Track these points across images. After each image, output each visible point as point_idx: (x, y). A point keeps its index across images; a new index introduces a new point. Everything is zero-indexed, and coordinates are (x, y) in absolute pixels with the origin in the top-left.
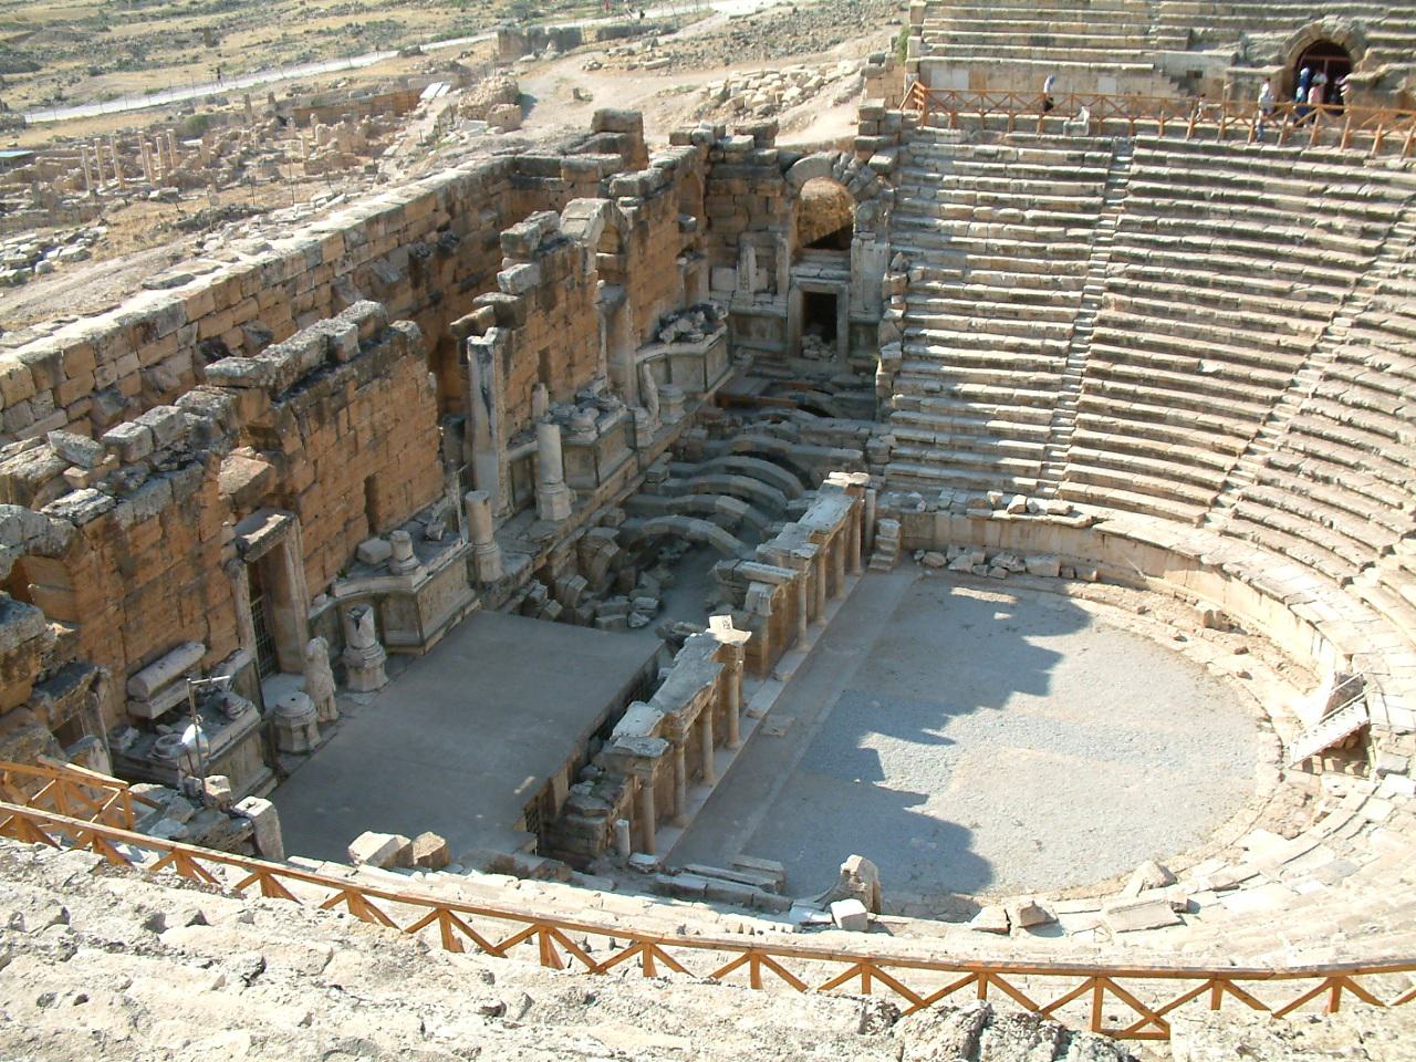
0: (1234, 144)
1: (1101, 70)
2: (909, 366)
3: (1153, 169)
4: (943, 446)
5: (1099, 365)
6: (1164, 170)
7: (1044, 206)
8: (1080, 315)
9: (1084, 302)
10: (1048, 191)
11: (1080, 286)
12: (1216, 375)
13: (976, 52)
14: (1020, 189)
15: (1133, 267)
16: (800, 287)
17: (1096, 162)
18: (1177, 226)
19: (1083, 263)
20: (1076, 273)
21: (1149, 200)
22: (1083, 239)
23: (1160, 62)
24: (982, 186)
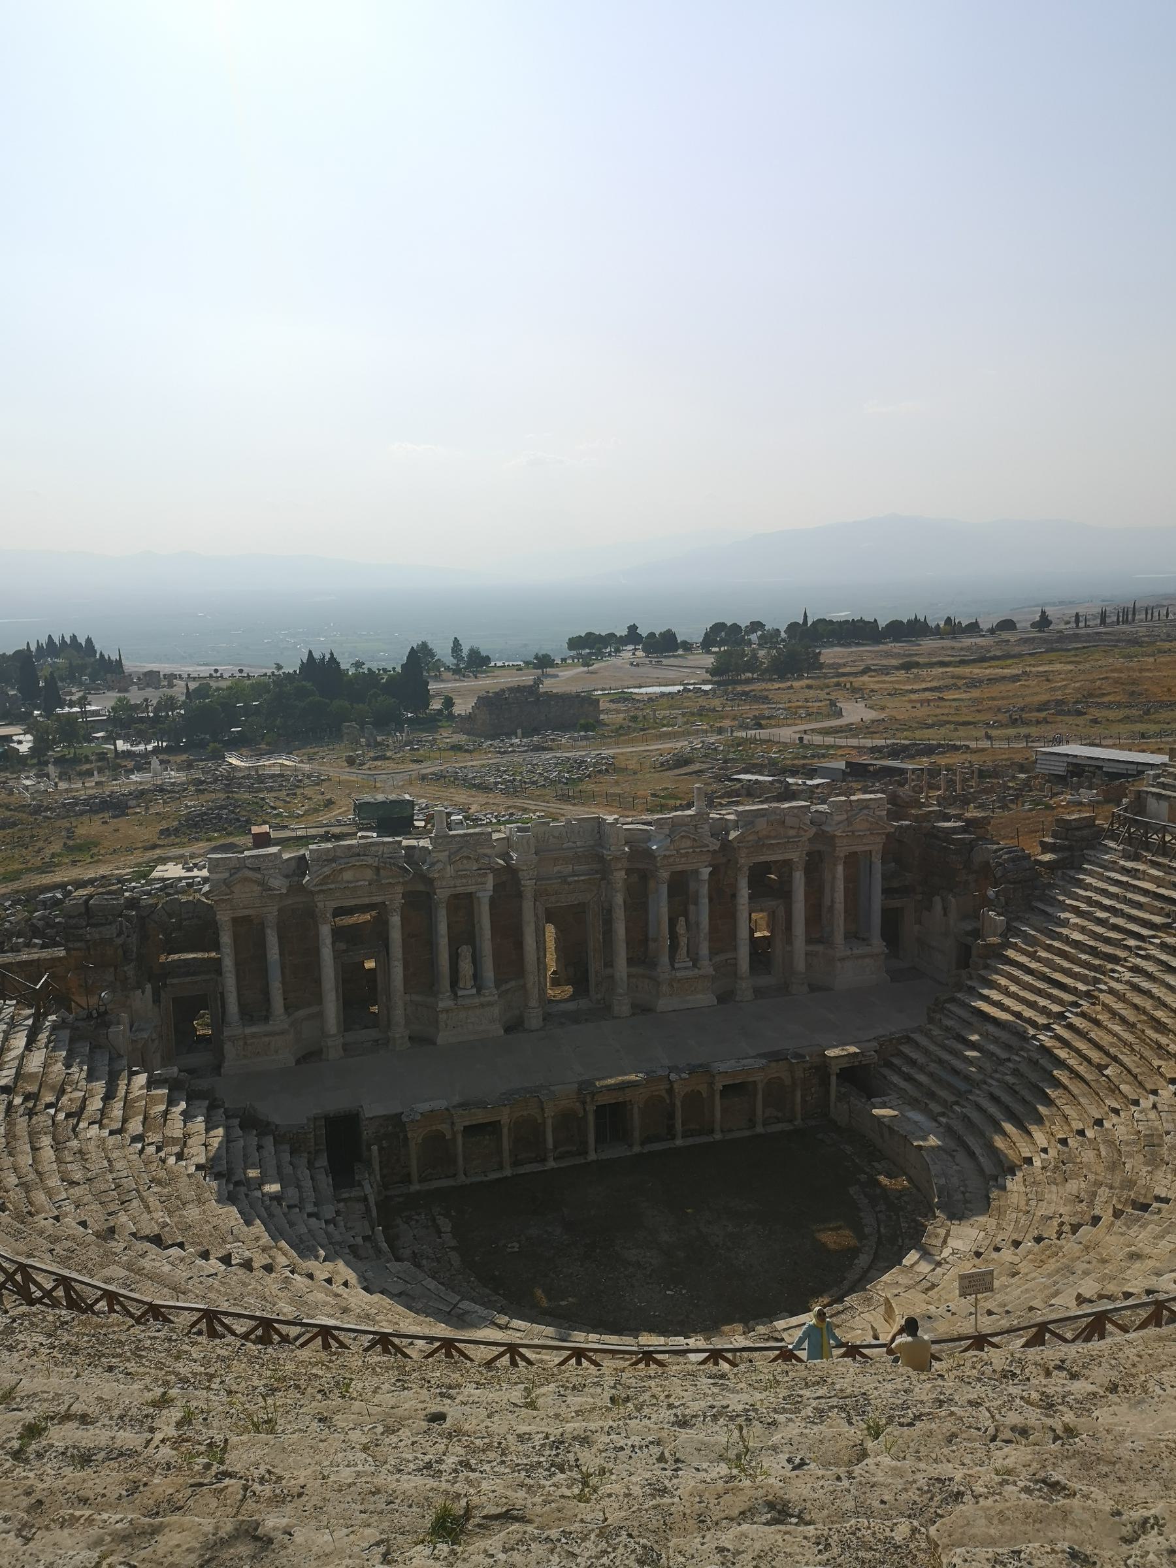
9: (1088, 995)
10: (1139, 906)
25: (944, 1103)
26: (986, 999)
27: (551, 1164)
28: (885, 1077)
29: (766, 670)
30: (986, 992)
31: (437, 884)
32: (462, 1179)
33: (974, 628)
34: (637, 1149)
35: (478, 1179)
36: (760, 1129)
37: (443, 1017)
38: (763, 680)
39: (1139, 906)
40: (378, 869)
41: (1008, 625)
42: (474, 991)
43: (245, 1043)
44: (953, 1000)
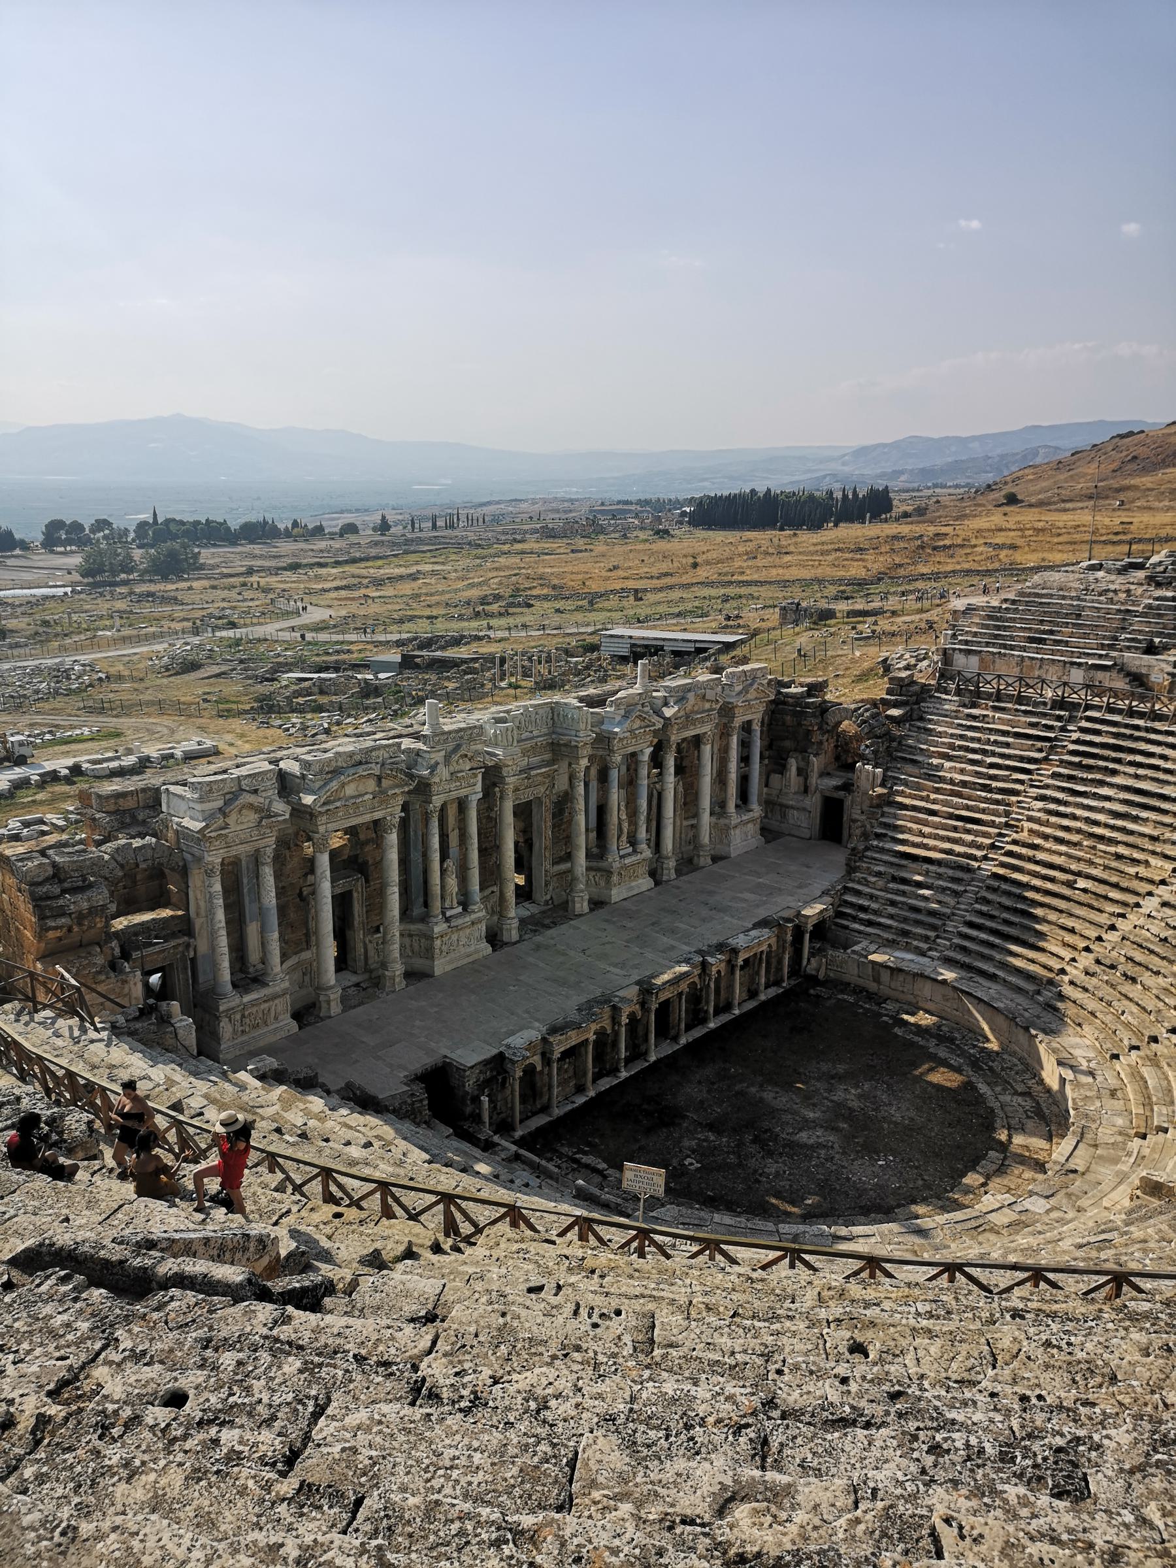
0: (1158, 725)
1: (1073, 663)
2: (869, 853)
3: (1088, 738)
4: (875, 912)
5: (1001, 871)
6: (1097, 739)
7: (1002, 756)
8: (1000, 835)
9: (1007, 825)
10: (1008, 745)
11: (1007, 814)
12: (1085, 891)
13: (987, 644)
14: (988, 742)
15: (1052, 806)
16: (822, 791)
17: (1050, 728)
18: (1092, 780)
19: (1014, 799)
20: (1008, 805)
21: (1077, 759)
22: (1021, 782)
23: (1119, 661)
24: (962, 737)
25: (926, 939)
26: (903, 842)
27: (624, 1074)
28: (846, 927)
29: (146, 571)
30: (901, 836)
31: (434, 789)
32: (557, 1112)
33: (319, 531)
34: (683, 1041)
35: (569, 1107)
36: (763, 997)
37: (438, 943)
38: (144, 581)
39: (1008, 745)
40: (379, 779)
41: (351, 529)
42: (460, 909)
43: (243, 1016)
44: (867, 849)
